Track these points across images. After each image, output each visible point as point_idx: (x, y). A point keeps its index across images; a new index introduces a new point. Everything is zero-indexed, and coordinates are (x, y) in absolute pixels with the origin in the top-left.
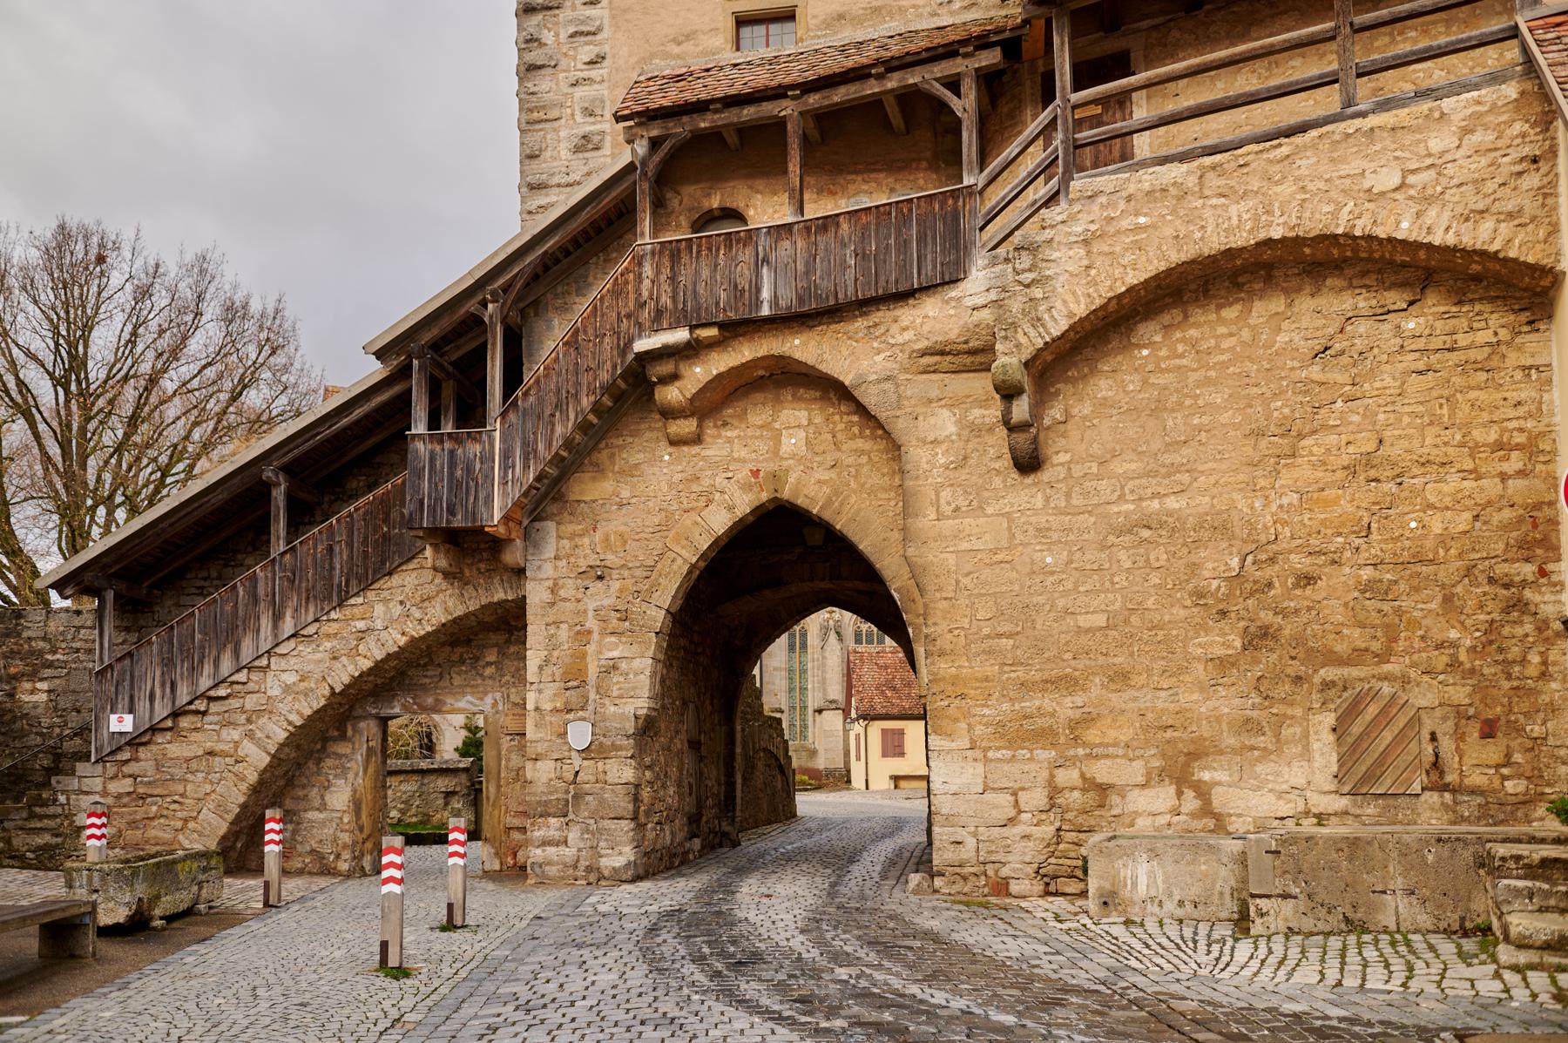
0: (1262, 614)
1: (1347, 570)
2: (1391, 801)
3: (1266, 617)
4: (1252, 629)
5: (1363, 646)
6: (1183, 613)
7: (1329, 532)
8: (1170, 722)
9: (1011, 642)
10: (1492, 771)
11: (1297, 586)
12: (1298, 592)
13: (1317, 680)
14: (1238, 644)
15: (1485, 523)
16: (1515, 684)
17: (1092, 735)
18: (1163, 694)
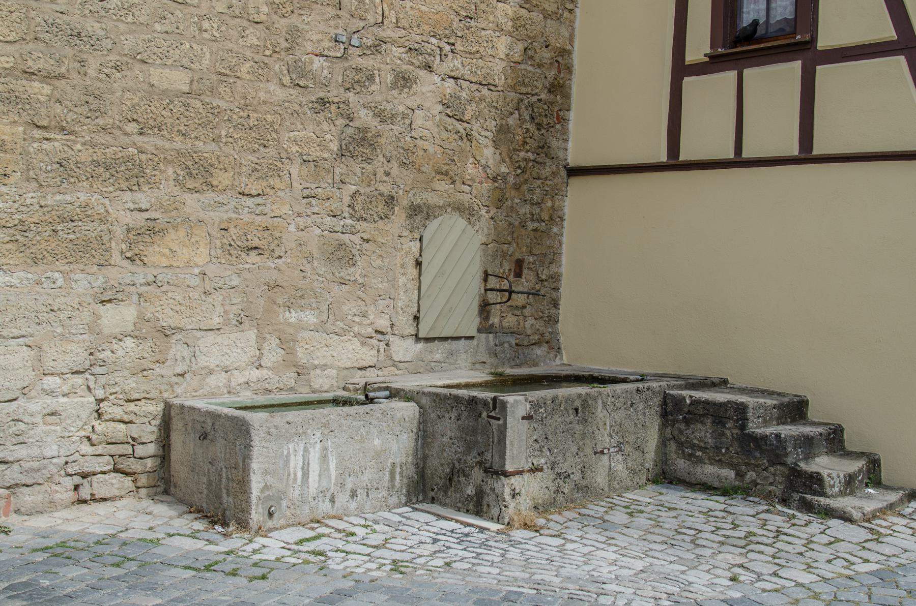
0: (363, 112)
1: (437, 79)
2: (454, 345)
3: (365, 117)
4: (350, 131)
5: (446, 168)
6: (280, 94)
7: (427, 28)
8: (256, 242)
9: (47, 89)
10: (519, 313)
11: (394, 86)
12: (395, 93)
13: (405, 203)
14: (334, 146)
15: (531, 58)
16: (536, 225)
17: (155, 253)
18: (250, 202)
